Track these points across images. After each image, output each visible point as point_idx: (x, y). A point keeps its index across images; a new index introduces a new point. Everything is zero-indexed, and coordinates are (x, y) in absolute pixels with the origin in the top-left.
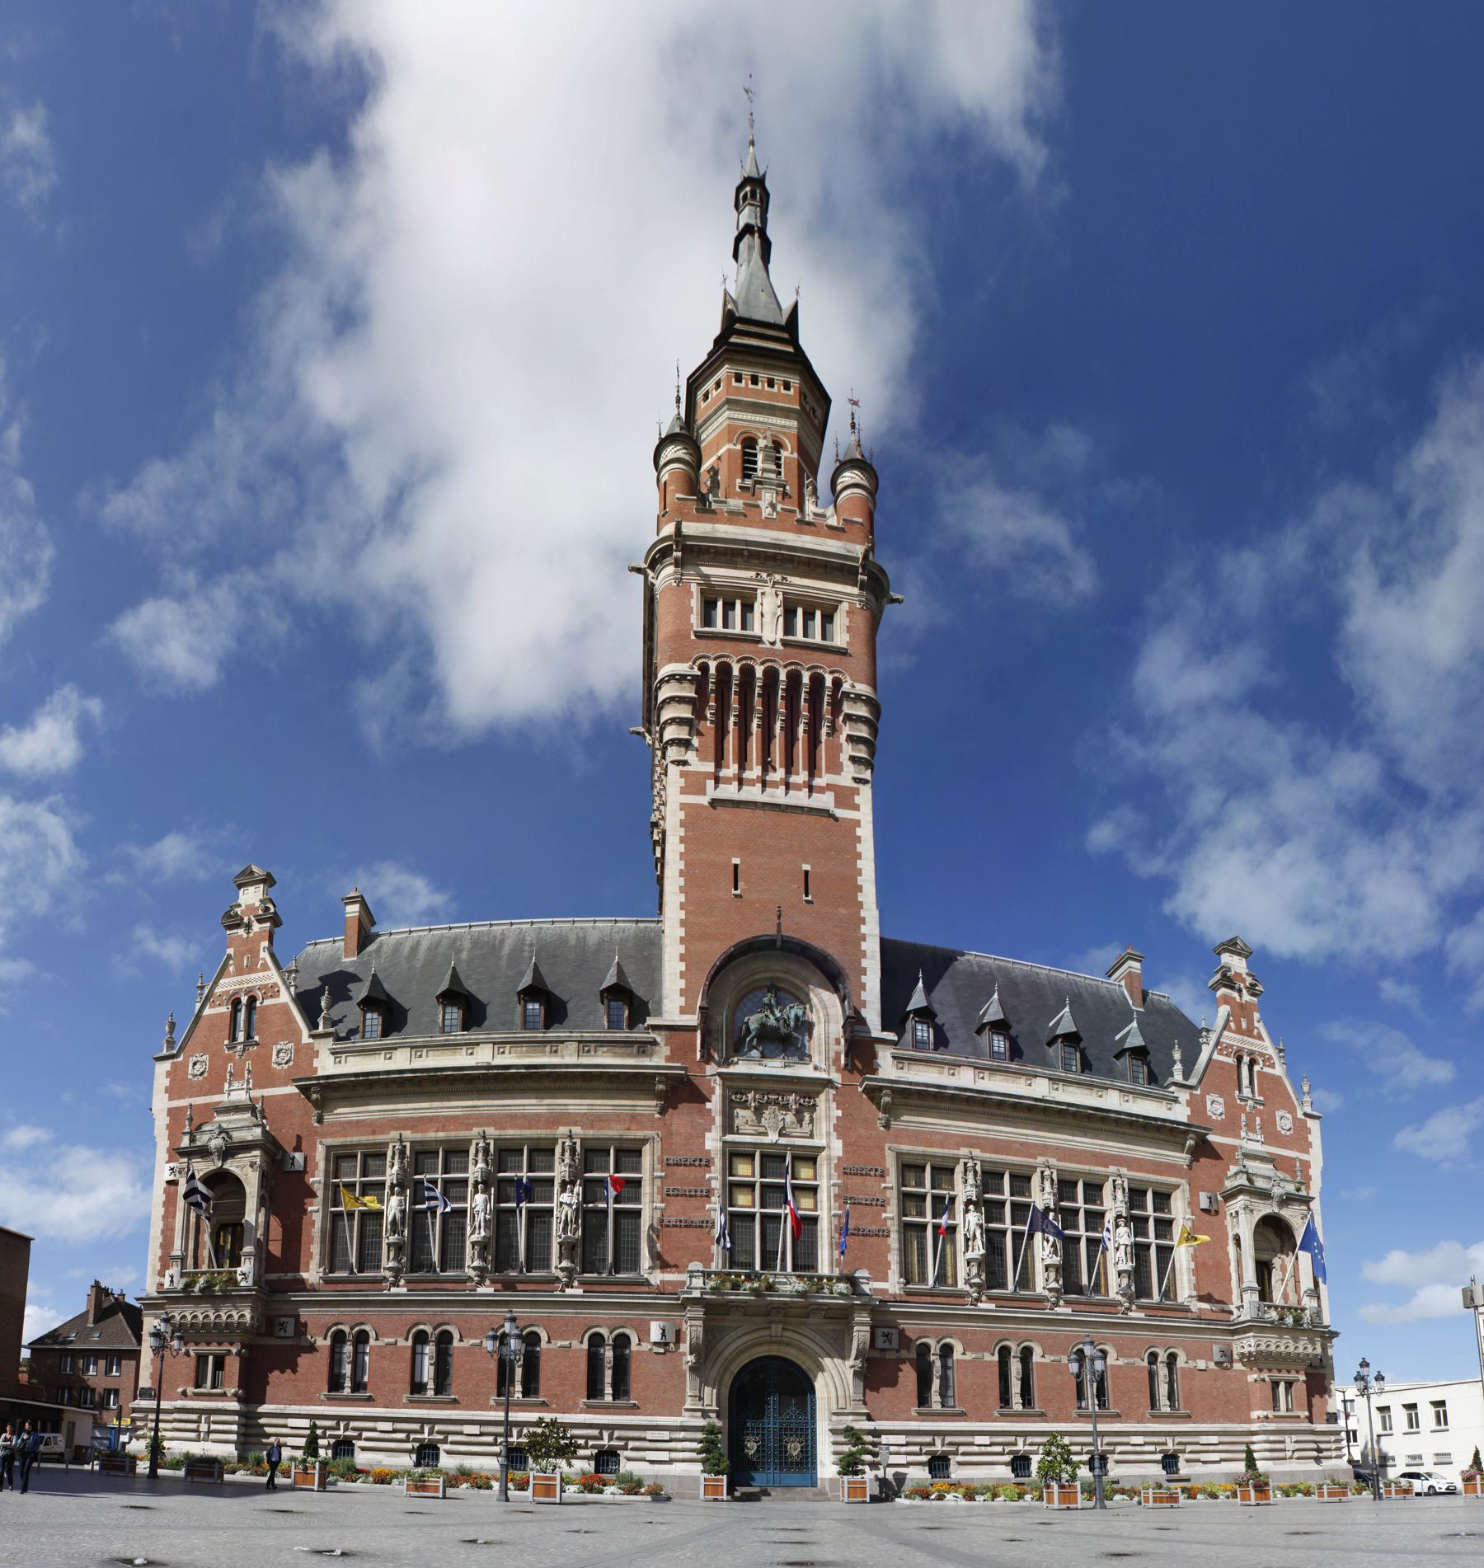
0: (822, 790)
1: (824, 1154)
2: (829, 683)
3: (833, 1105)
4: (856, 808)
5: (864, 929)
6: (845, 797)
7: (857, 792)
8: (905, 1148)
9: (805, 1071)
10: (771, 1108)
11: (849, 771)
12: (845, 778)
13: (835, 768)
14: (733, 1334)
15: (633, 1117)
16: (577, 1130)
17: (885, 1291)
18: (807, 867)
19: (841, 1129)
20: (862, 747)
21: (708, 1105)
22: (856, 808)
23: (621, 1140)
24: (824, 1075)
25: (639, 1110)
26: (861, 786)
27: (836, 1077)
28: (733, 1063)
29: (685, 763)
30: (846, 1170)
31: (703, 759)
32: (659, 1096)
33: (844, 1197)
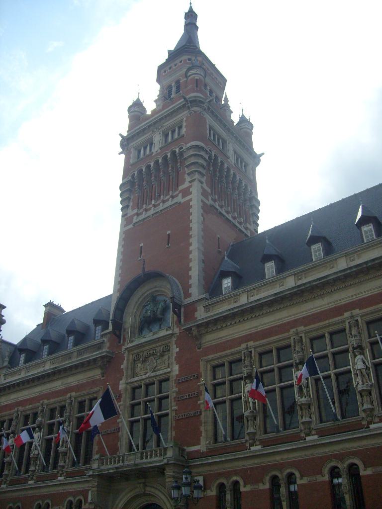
0: (177, 195)
1: (171, 374)
2: (177, 150)
3: (175, 346)
4: (191, 193)
5: (191, 248)
6: (186, 192)
7: (191, 186)
8: (210, 357)
9: (163, 333)
10: (150, 358)
11: (188, 179)
12: (186, 185)
13: (184, 182)
14: (124, 493)
15: (93, 381)
16: (73, 394)
17: (198, 451)
18: (169, 232)
19: (178, 360)
20: (193, 167)
21: (122, 367)
22: (191, 193)
23: (88, 394)
24: (170, 332)
25: (97, 377)
26: (193, 183)
27: (177, 330)
28: (132, 341)
29: (126, 214)
30: (179, 383)
31: (133, 209)
32: (101, 367)
33: (178, 400)
